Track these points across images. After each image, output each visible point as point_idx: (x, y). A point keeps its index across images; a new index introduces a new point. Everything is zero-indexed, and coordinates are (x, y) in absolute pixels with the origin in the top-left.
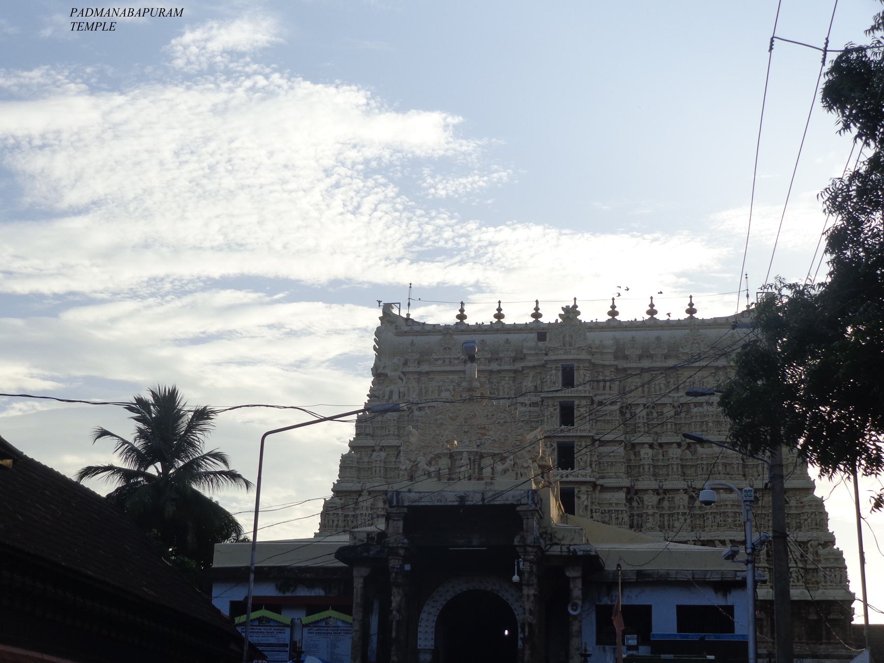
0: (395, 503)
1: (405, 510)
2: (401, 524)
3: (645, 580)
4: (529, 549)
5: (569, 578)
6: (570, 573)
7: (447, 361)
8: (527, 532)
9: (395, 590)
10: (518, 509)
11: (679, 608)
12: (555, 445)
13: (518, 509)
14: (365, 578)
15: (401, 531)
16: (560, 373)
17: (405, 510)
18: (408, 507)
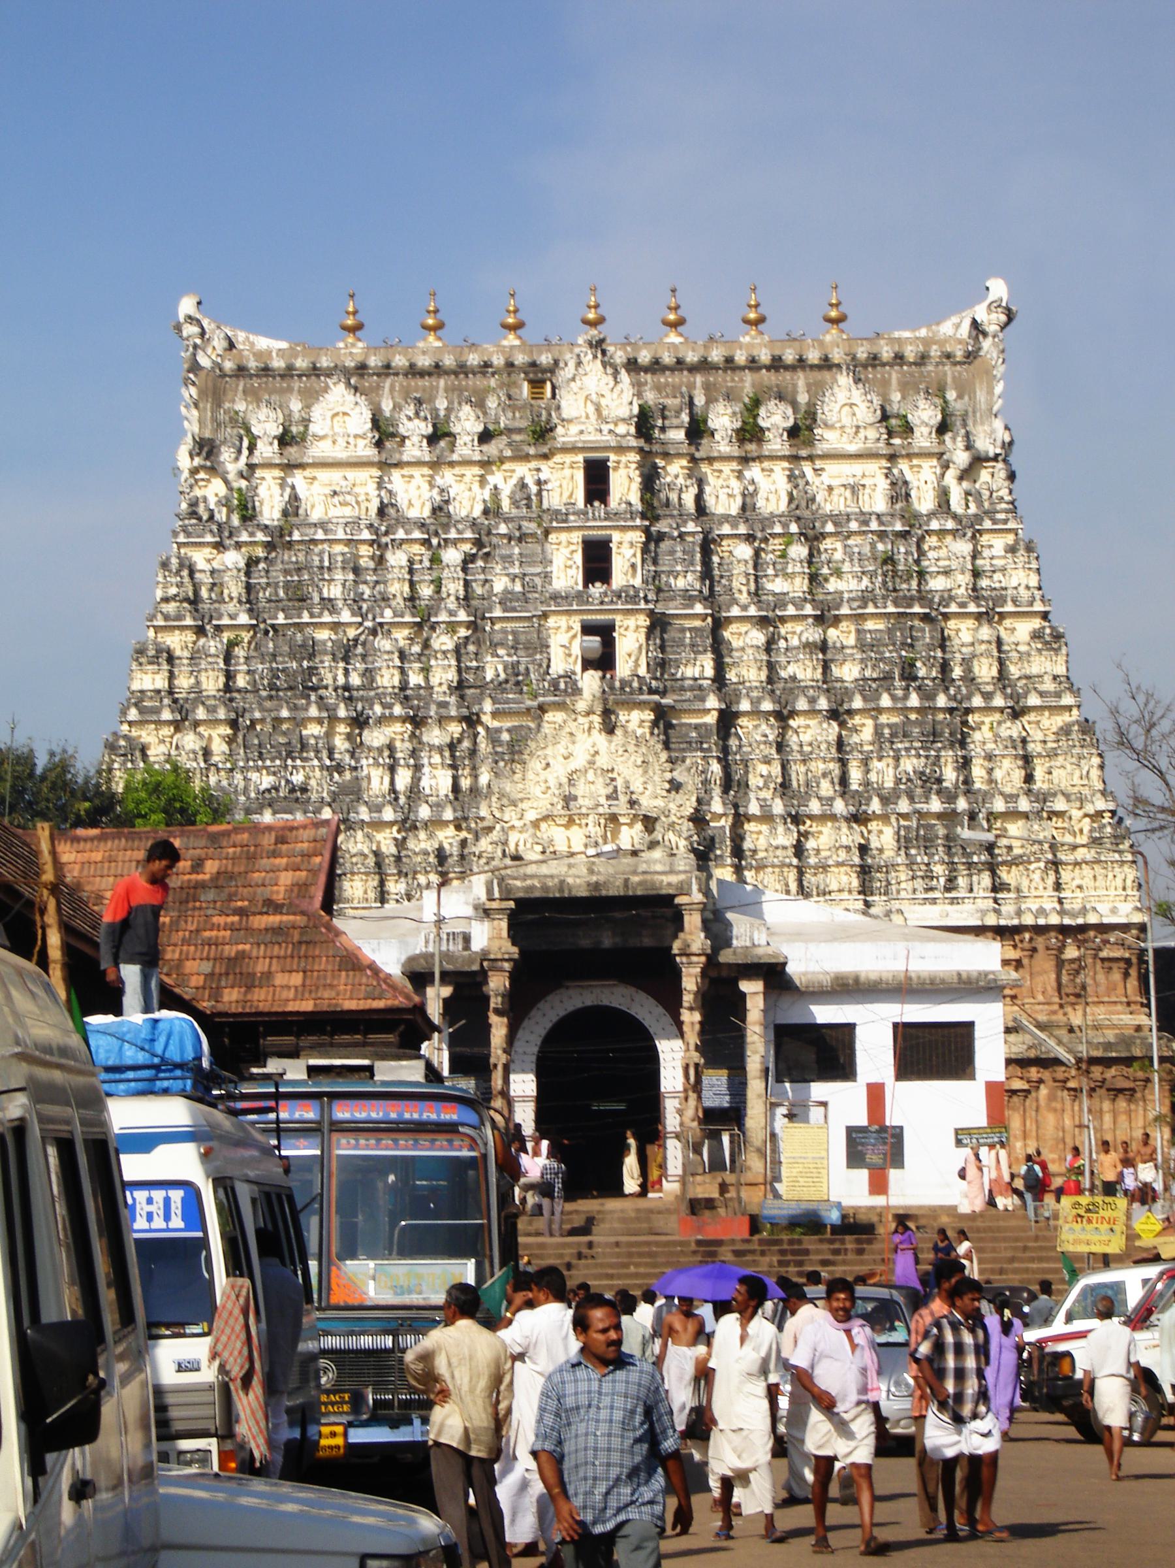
0: (497, 895)
1: (512, 904)
2: (504, 925)
3: (849, 988)
4: (695, 959)
5: (743, 996)
6: (746, 986)
7: (341, 441)
8: (691, 933)
9: (494, 1019)
10: (678, 900)
11: (896, 1026)
12: (577, 627)
13: (678, 900)
14: (445, 1001)
15: (505, 933)
16: (580, 476)
17: (512, 904)
18: (516, 900)
